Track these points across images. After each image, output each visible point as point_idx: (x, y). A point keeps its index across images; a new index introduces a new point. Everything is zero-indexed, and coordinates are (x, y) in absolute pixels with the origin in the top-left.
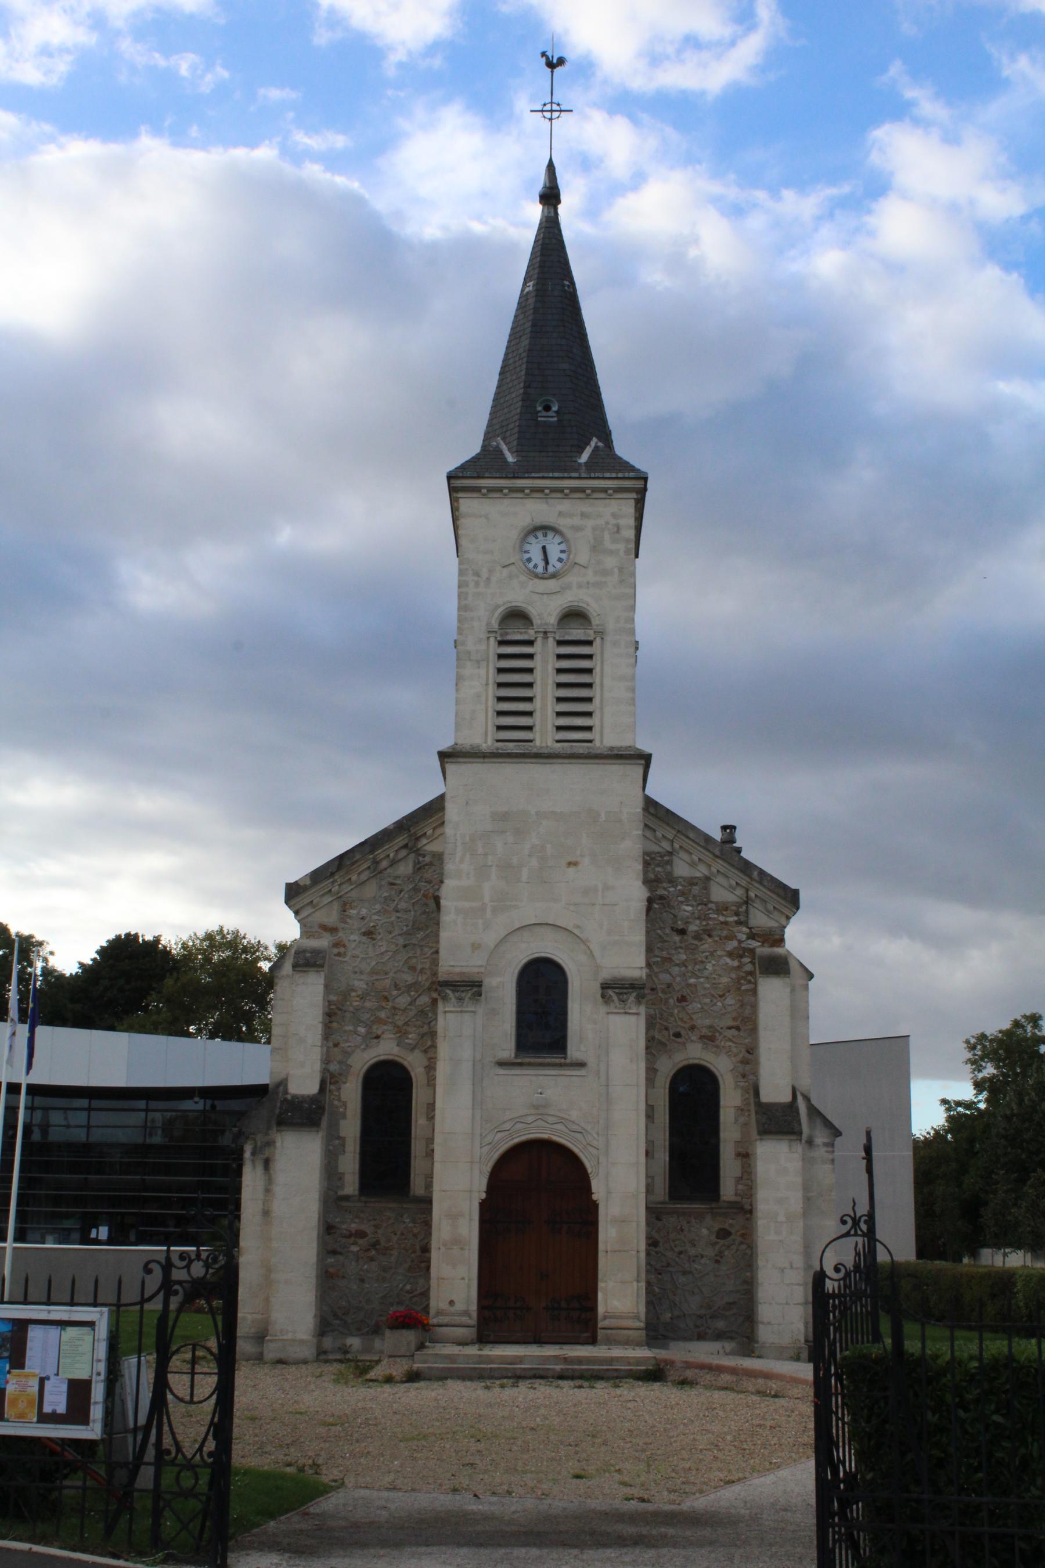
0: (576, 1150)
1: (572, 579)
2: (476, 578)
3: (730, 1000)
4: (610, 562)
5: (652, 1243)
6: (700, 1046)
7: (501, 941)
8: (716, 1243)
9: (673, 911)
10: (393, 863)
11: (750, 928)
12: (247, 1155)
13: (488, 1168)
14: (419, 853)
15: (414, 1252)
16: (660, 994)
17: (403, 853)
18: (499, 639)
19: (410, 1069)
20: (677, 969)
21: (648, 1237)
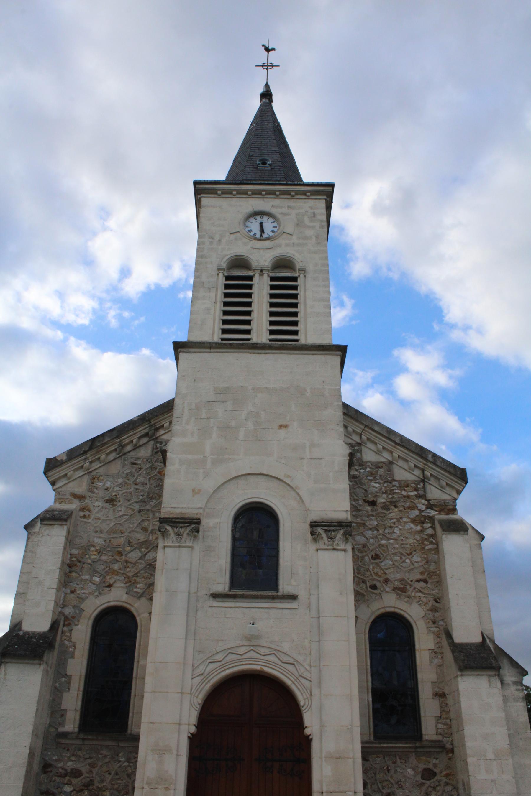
0: (289, 683)
2: (210, 240)
3: (416, 558)
4: (309, 233)
6: (393, 596)
7: (219, 488)
8: (422, 784)
9: (364, 487)
10: (136, 447)
11: (428, 501)
13: (199, 699)
17: (145, 440)
18: (226, 274)
19: (135, 614)
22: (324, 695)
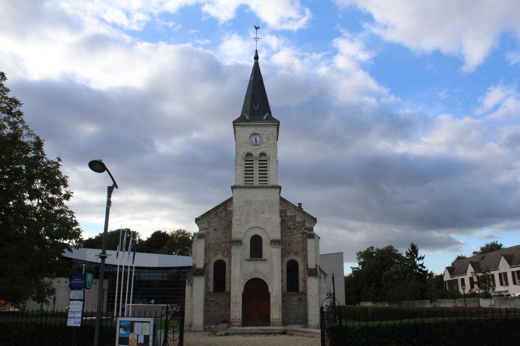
1: (262, 146)
3: (300, 244)
4: (271, 142)
5: (283, 302)
10: (221, 213)
12: (187, 282)
14: (227, 210)
21: (282, 300)
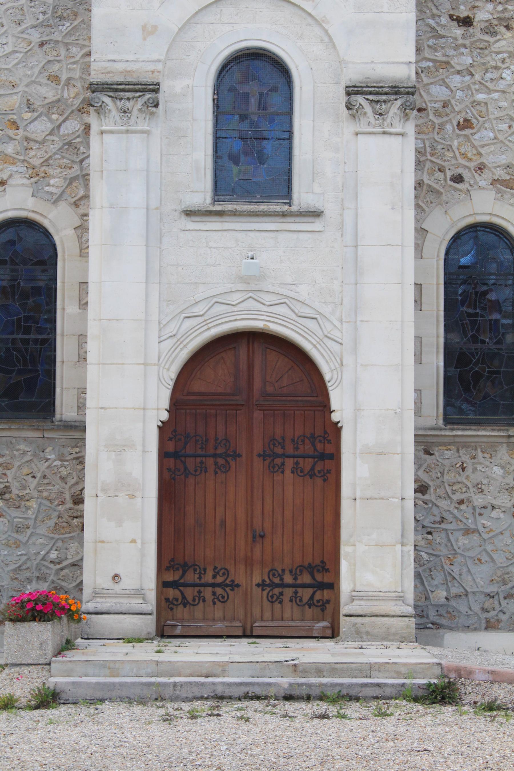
7: (188, 22)
13: (172, 373)
15: (63, 503)
16: (431, 117)
19: (51, 230)
20: (457, 78)
22: (361, 365)
